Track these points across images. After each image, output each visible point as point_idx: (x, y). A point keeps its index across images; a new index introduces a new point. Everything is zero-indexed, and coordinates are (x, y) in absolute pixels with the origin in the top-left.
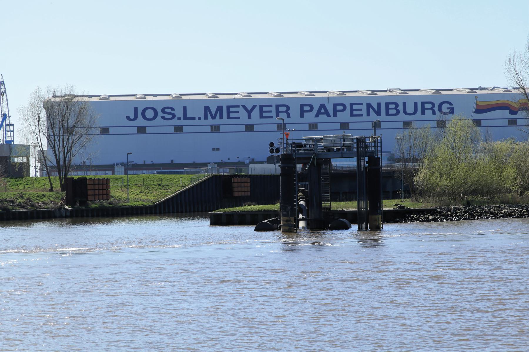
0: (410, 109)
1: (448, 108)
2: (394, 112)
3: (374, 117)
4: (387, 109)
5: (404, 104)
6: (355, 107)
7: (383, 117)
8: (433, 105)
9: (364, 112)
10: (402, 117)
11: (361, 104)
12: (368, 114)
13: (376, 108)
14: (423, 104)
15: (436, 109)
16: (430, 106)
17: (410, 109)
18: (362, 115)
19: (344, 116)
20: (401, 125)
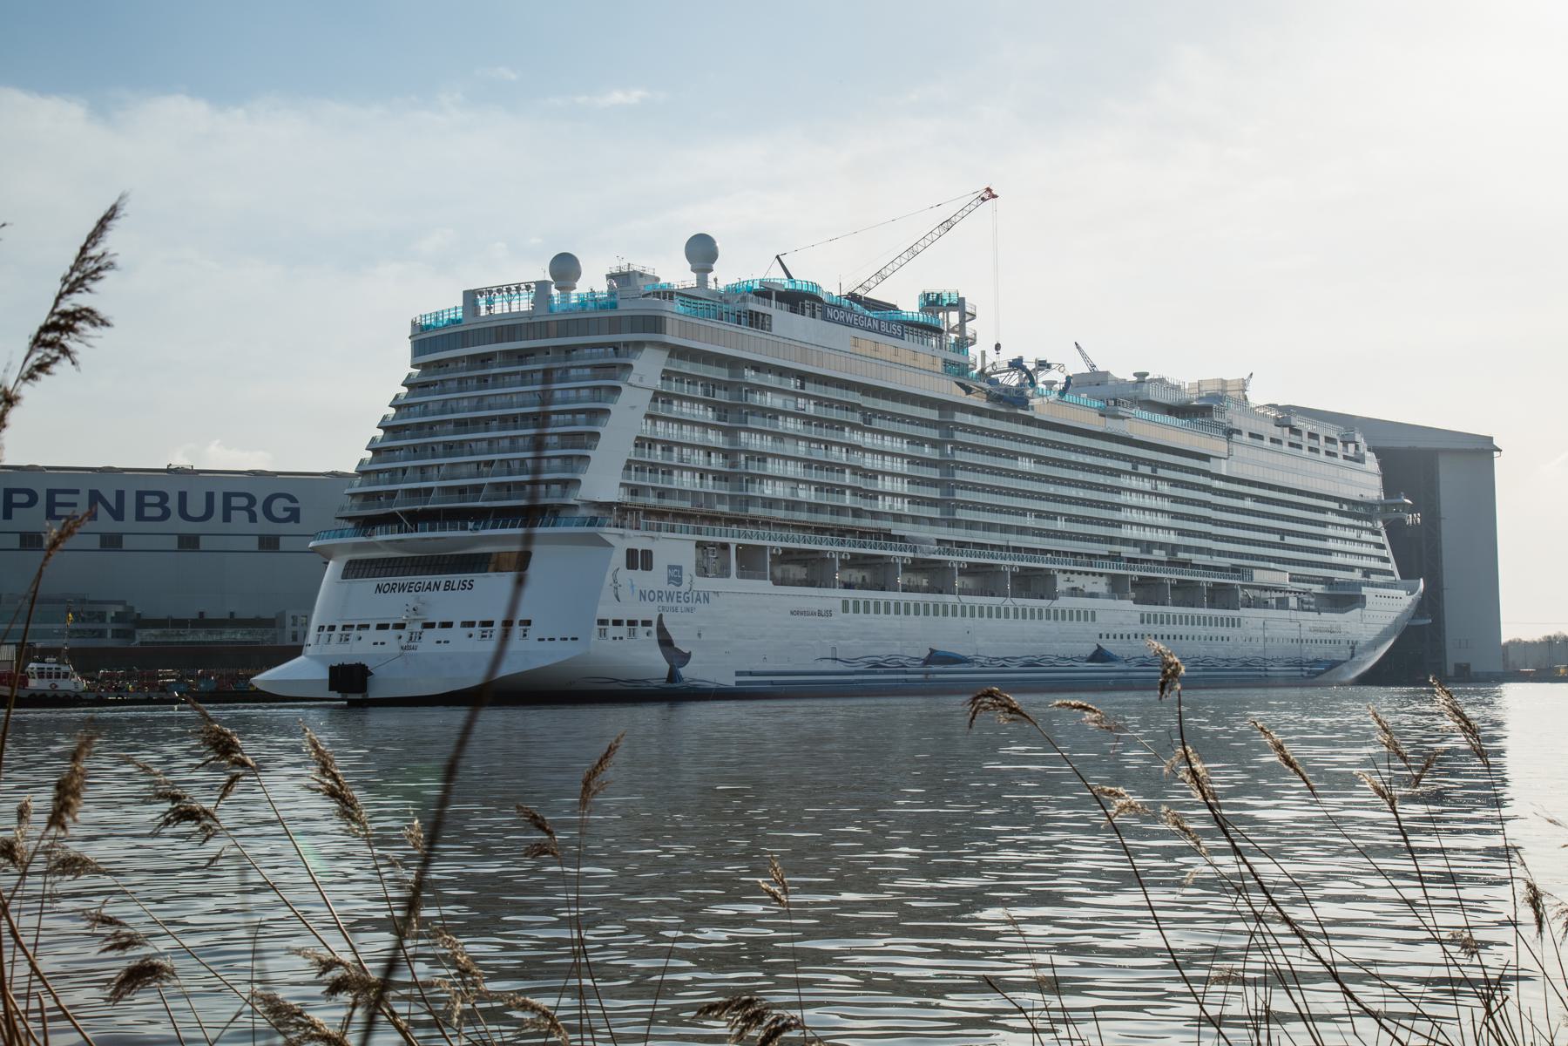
0: (196, 507)
1: (286, 509)
2: (157, 512)
5: (183, 496)
6: (59, 498)
7: (129, 523)
8: (252, 500)
10: (177, 524)
11: (77, 492)
12: (93, 516)
13: (112, 501)
14: (227, 496)
15: (258, 509)
16: (244, 502)
17: (196, 507)
19: (31, 519)
20: (173, 543)
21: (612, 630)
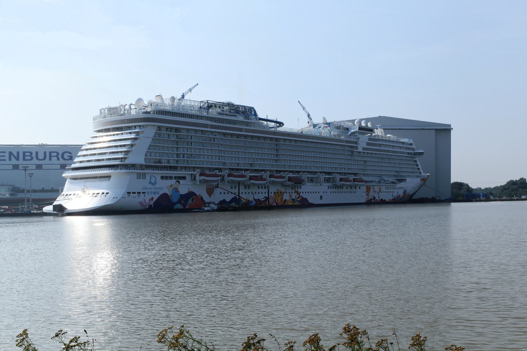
0: (41, 156)
2: (29, 158)
3: (14, 161)
4: (24, 156)
5: (37, 153)
7: (21, 161)
8: (58, 154)
9: (7, 158)
10: (35, 161)
11: (5, 152)
12: (10, 159)
13: (16, 155)
14: (50, 153)
15: (60, 156)
17: (41, 156)
18: (5, 160)
21: (132, 195)
